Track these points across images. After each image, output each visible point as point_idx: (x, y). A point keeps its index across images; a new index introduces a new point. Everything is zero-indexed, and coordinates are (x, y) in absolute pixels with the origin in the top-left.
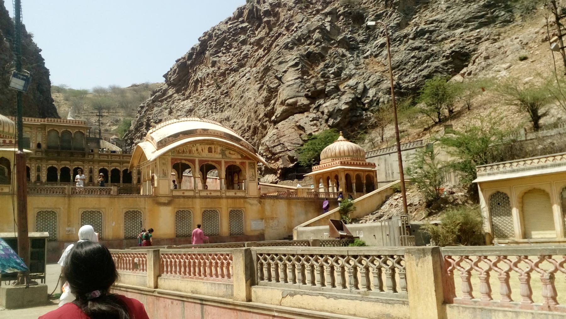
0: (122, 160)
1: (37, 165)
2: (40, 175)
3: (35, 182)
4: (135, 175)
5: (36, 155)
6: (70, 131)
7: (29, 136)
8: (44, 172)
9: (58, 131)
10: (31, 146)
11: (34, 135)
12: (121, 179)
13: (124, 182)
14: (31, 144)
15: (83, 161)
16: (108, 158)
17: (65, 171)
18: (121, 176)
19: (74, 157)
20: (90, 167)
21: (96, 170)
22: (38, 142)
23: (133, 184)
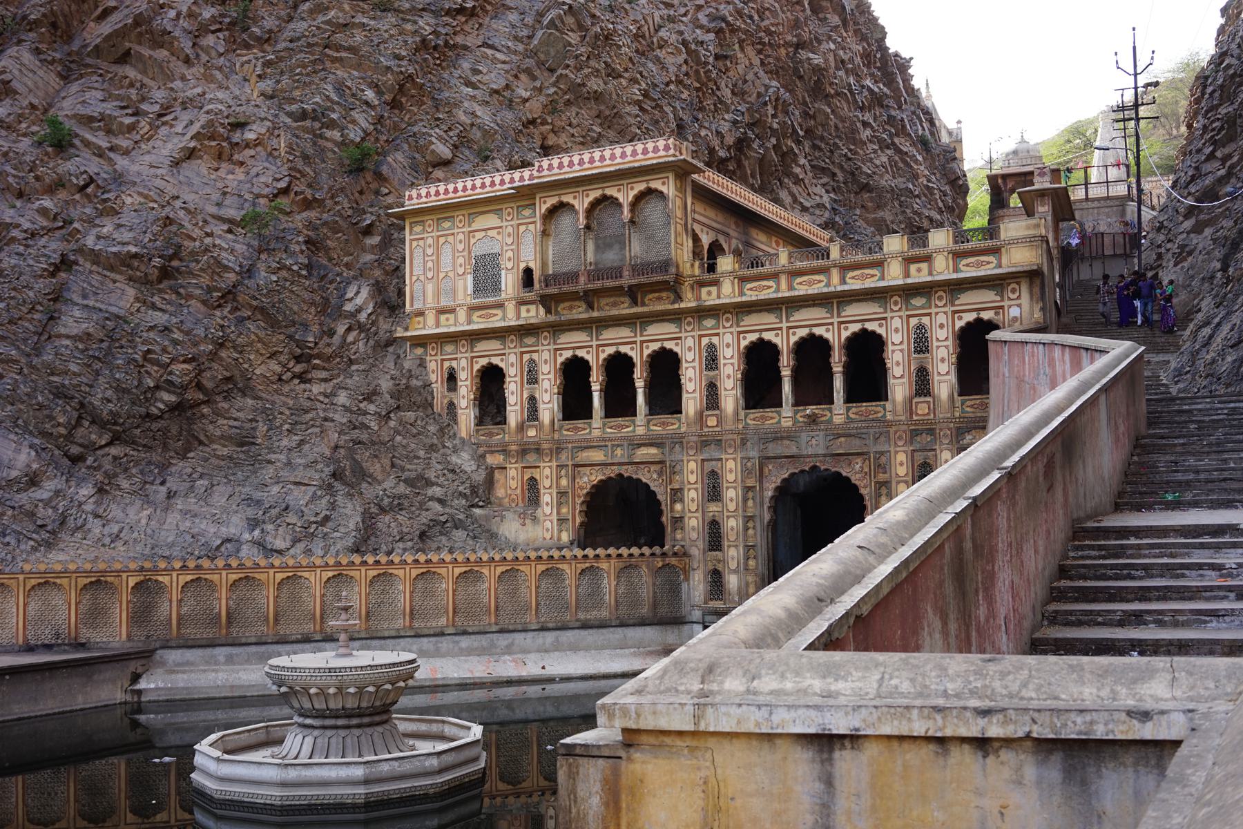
0: (839, 288)
1: (526, 357)
2: (537, 396)
3: (521, 428)
4: (898, 356)
5: (438, 325)
6: (616, 194)
7: (497, 249)
8: (546, 384)
9: (575, 203)
10: (503, 288)
11: (509, 241)
12: (838, 383)
13: (850, 398)
14: (503, 273)
15: (676, 317)
16: (504, 319)
17: (619, 366)
18: (838, 369)
19: (643, 304)
20: (705, 341)
21: (728, 352)
22: (523, 266)
23: (894, 401)
